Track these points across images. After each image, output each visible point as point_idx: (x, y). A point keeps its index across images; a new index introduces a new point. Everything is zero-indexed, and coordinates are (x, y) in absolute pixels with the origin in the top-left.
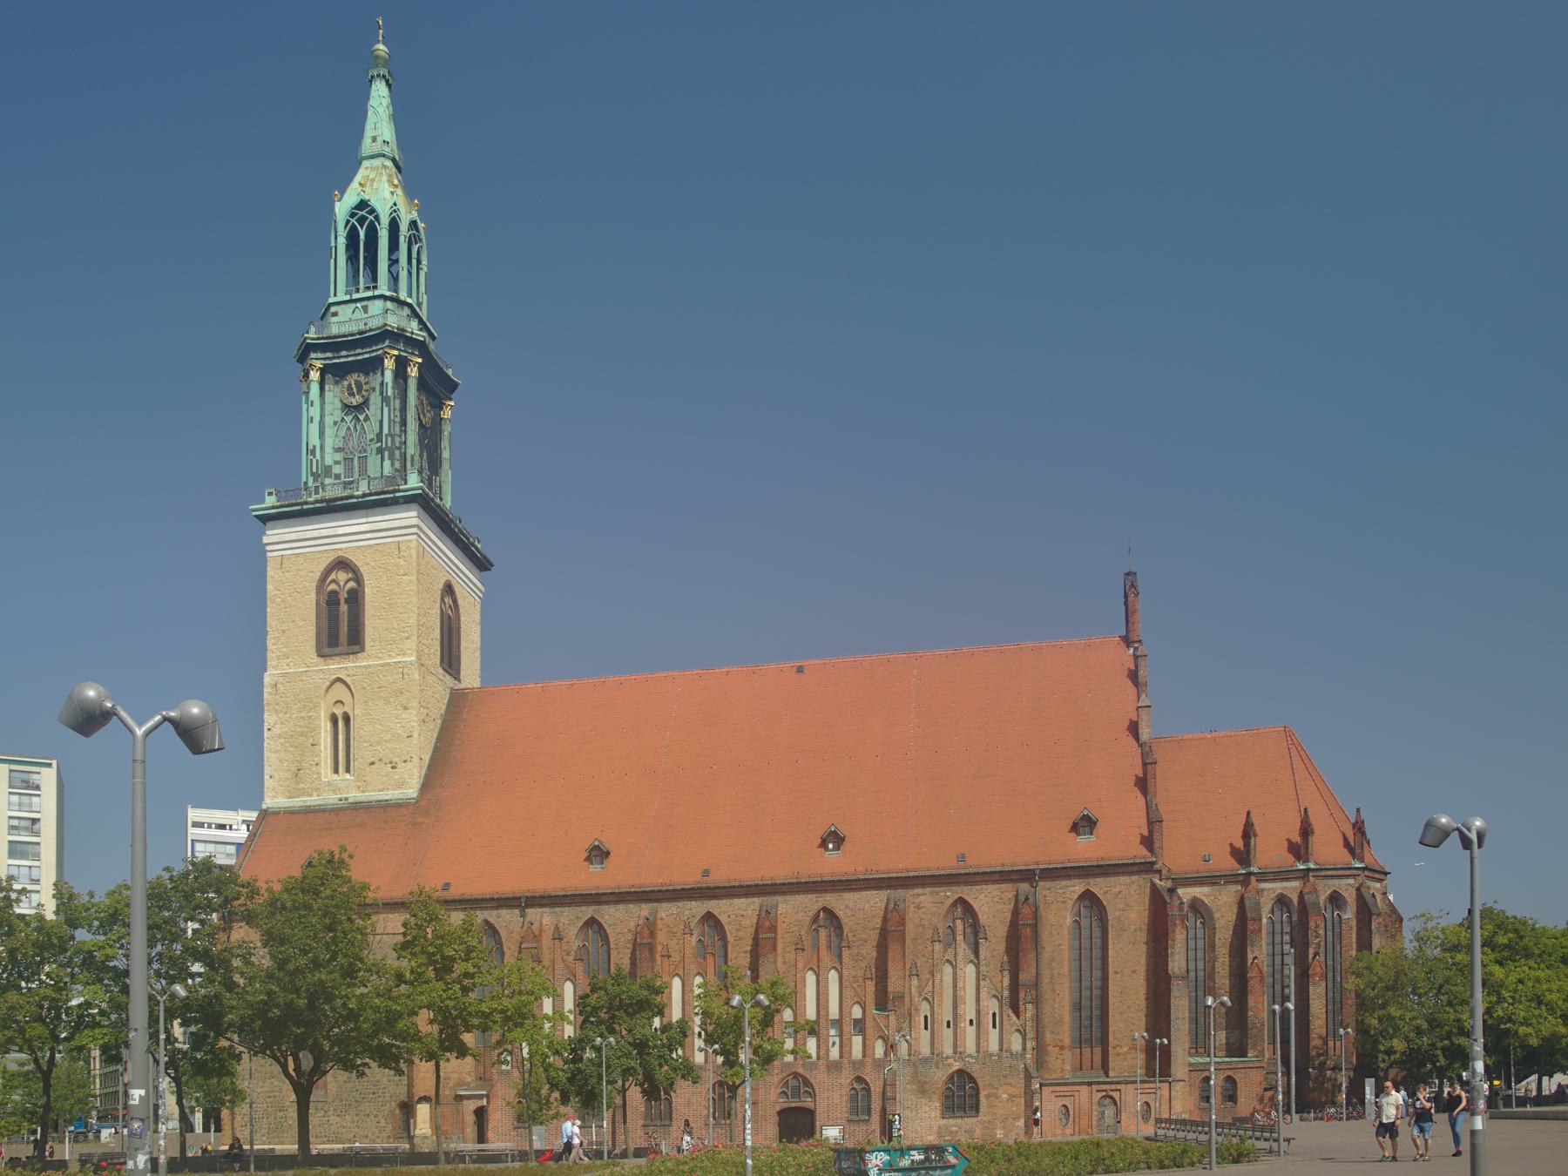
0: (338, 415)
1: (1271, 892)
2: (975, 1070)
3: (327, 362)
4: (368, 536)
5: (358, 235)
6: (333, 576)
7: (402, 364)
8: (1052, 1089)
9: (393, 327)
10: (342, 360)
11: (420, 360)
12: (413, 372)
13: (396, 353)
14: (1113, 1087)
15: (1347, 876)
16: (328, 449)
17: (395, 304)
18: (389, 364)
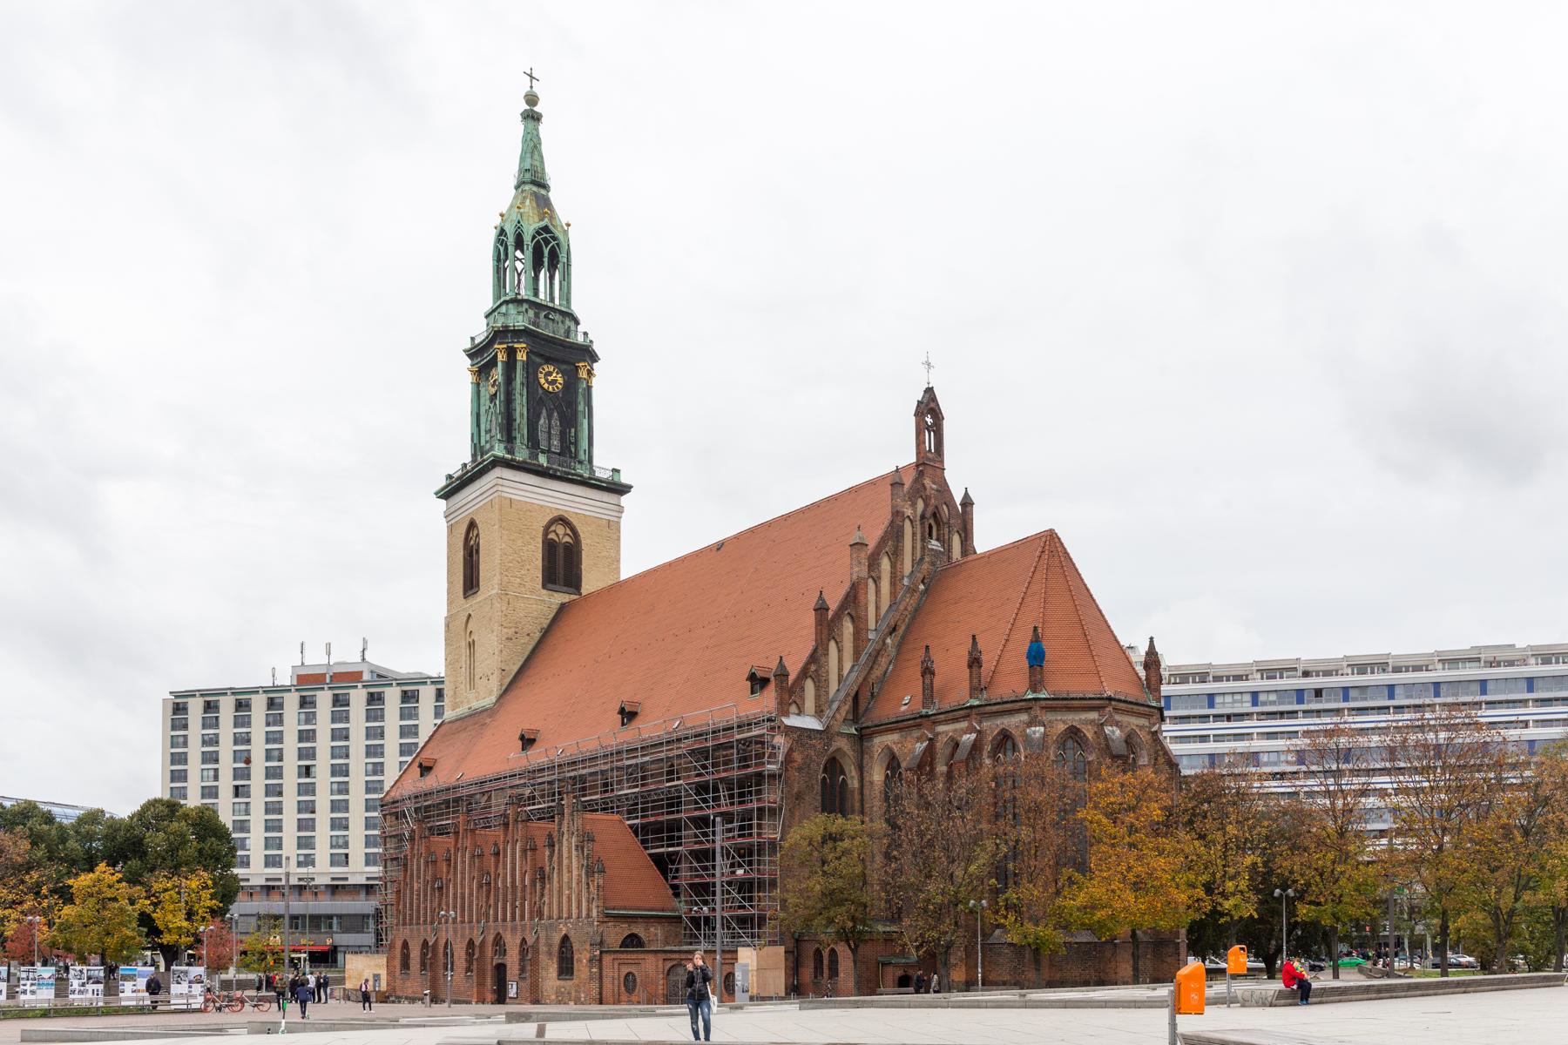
0: (488, 402)
1: (944, 736)
2: (572, 934)
3: (479, 365)
4: (480, 498)
5: (543, 254)
6: (471, 535)
7: (511, 352)
8: (613, 956)
9: (499, 327)
10: (485, 361)
11: (525, 346)
12: (521, 357)
13: (505, 346)
14: (683, 956)
15: (1019, 711)
16: (483, 433)
17: (516, 304)
18: (502, 357)
